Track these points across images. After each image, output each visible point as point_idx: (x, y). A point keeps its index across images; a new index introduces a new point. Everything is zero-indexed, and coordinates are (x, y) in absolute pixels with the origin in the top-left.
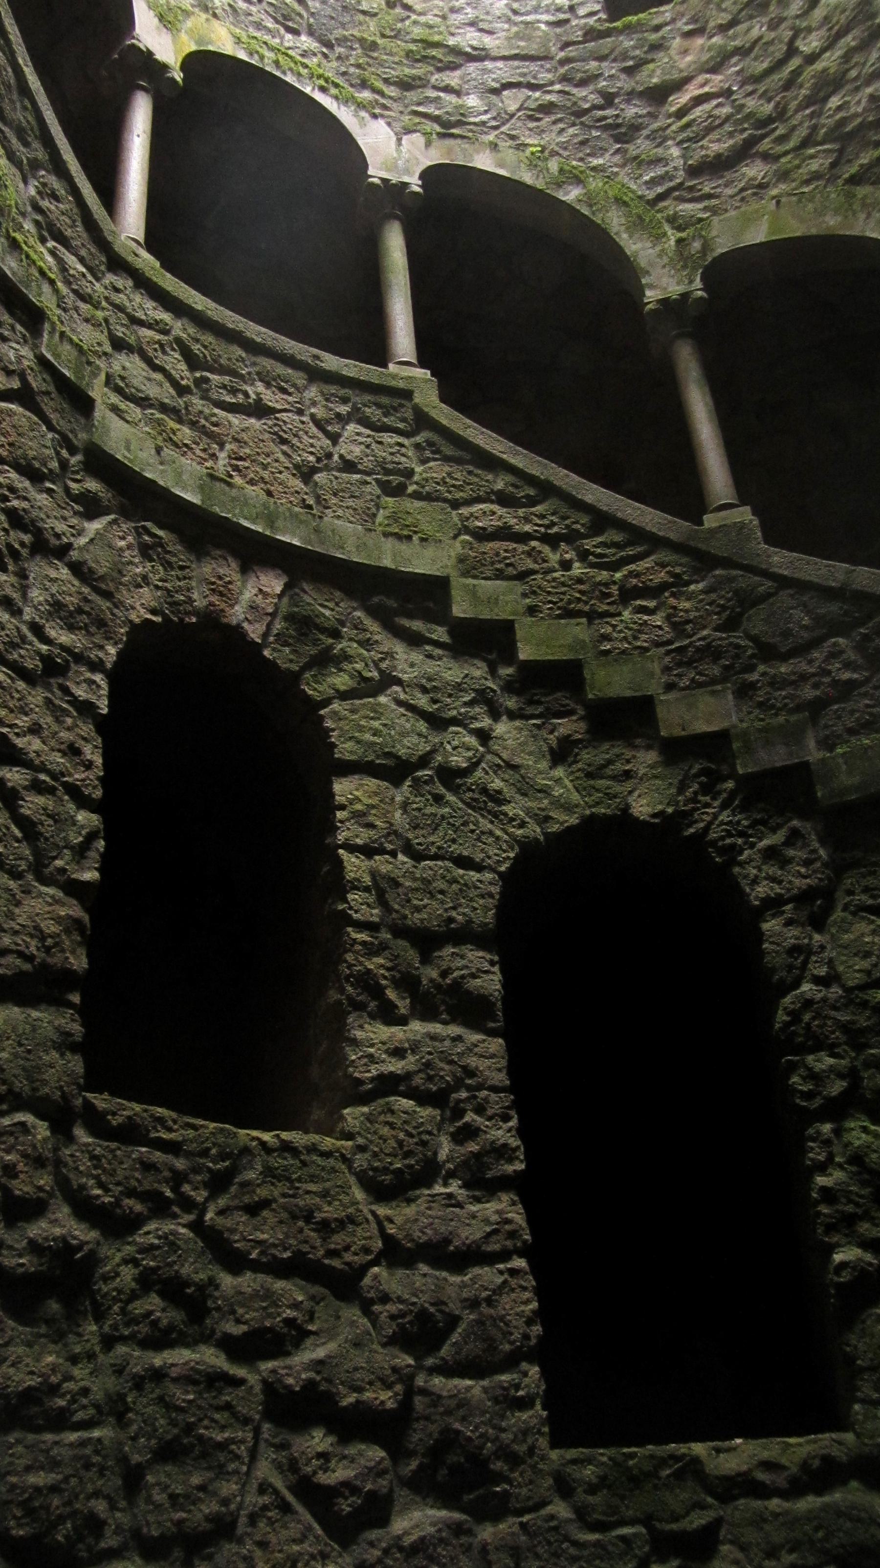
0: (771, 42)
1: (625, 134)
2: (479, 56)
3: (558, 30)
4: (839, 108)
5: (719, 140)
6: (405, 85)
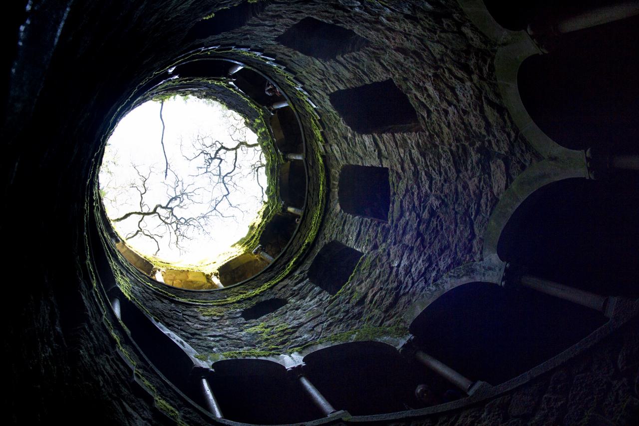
0: (384, 271)
1: (358, 317)
2: (301, 325)
4: (416, 270)
5: (387, 300)
6: (283, 343)
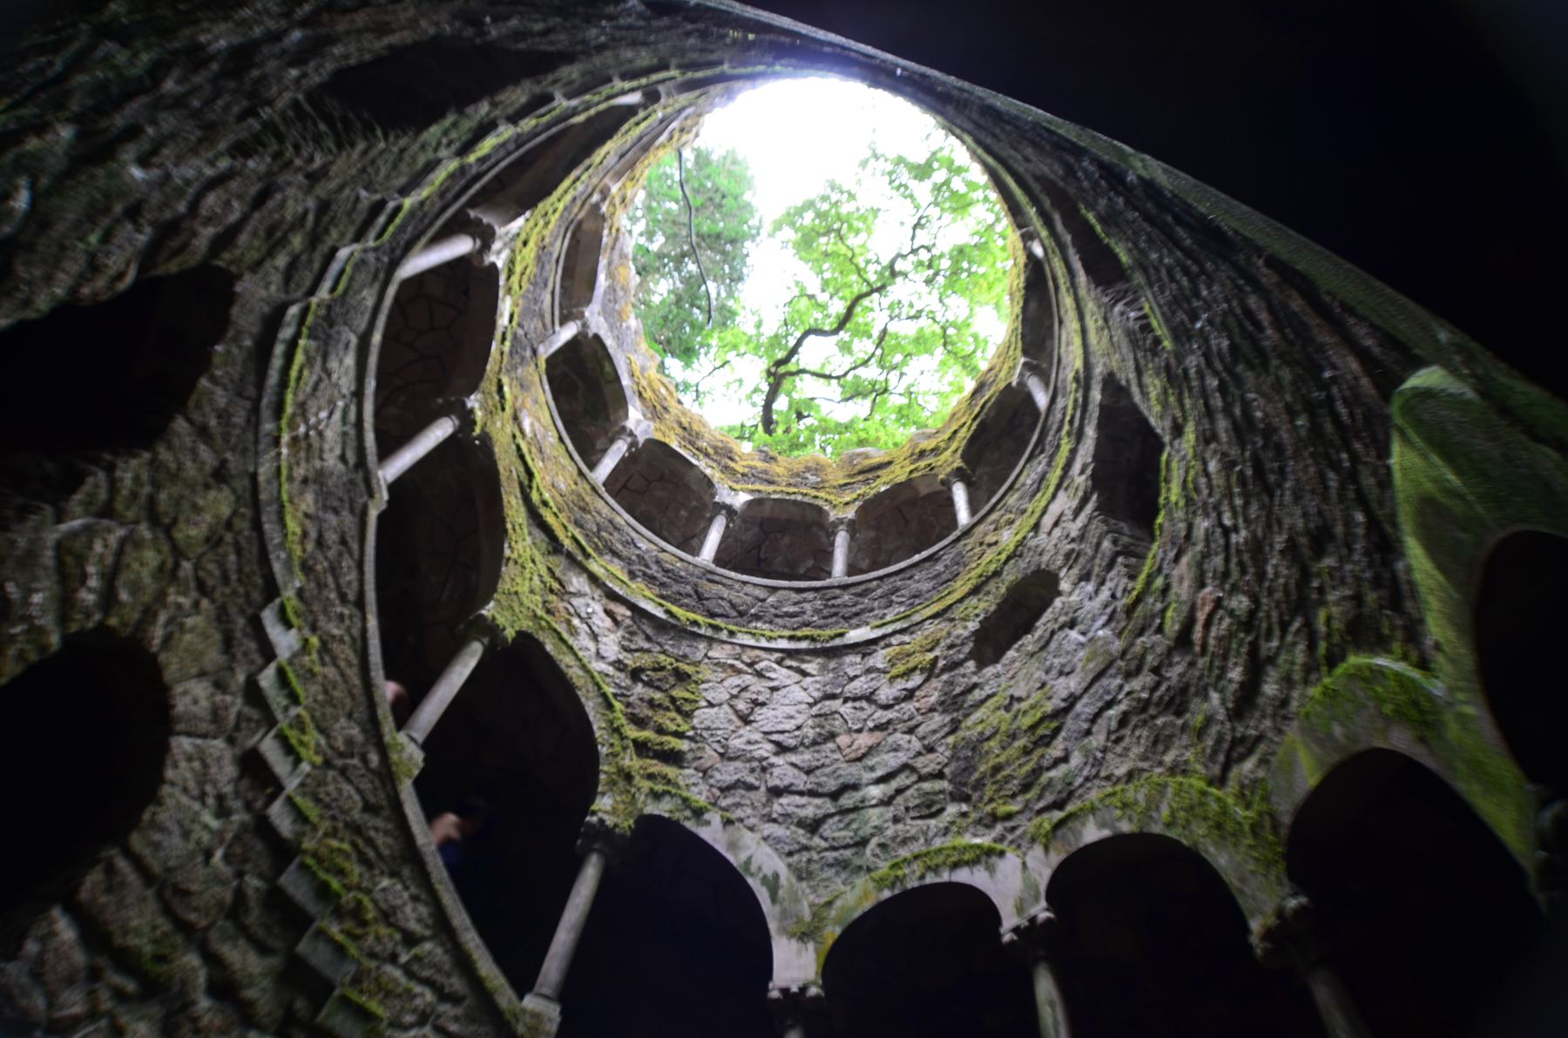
1: (1181, 704)
2: (1072, 700)
3: (1113, 624)
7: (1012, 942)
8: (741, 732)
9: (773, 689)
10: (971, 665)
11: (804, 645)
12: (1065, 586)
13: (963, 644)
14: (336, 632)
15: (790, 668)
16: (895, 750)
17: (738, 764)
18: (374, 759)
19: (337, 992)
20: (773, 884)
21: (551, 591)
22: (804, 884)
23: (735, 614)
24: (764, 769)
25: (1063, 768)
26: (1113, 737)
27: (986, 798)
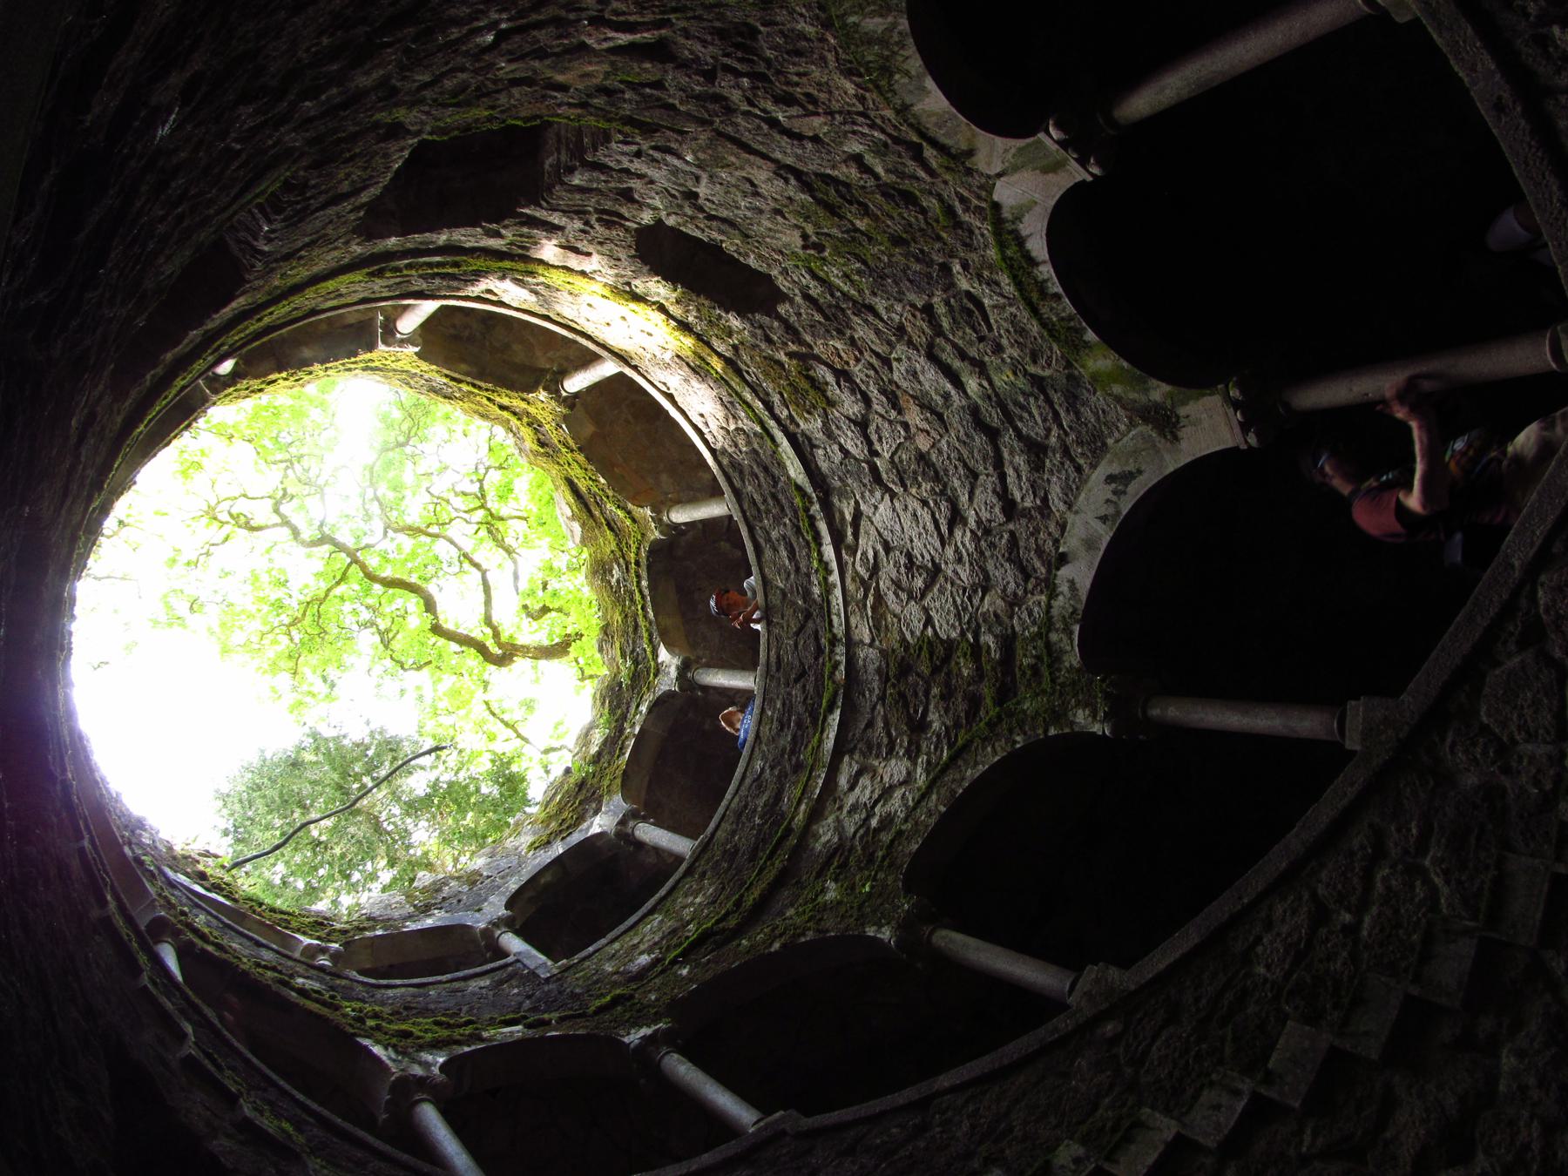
1: (741, 34)
2: (783, 171)
7: (1098, 163)
8: (950, 573)
9: (888, 548)
10: (782, 309)
11: (823, 527)
12: (647, 218)
13: (761, 327)
14: (966, 1125)
15: (856, 535)
16: (915, 374)
17: (990, 566)
18: (1110, 1028)
19: (1414, 991)
20: (1119, 480)
21: (843, 866)
22: (1110, 441)
23: (810, 624)
24: (987, 532)
25: (869, 159)
26: (811, 107)
27: (937, 246)
